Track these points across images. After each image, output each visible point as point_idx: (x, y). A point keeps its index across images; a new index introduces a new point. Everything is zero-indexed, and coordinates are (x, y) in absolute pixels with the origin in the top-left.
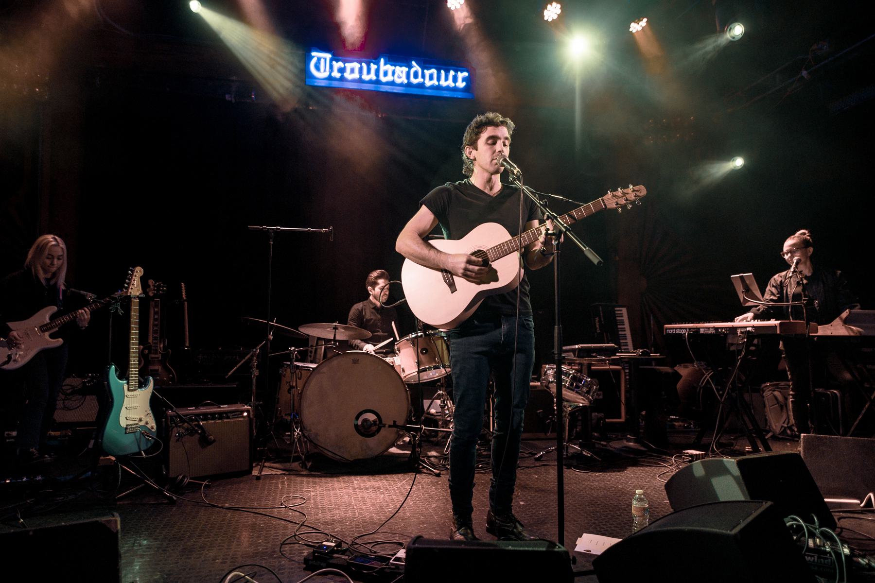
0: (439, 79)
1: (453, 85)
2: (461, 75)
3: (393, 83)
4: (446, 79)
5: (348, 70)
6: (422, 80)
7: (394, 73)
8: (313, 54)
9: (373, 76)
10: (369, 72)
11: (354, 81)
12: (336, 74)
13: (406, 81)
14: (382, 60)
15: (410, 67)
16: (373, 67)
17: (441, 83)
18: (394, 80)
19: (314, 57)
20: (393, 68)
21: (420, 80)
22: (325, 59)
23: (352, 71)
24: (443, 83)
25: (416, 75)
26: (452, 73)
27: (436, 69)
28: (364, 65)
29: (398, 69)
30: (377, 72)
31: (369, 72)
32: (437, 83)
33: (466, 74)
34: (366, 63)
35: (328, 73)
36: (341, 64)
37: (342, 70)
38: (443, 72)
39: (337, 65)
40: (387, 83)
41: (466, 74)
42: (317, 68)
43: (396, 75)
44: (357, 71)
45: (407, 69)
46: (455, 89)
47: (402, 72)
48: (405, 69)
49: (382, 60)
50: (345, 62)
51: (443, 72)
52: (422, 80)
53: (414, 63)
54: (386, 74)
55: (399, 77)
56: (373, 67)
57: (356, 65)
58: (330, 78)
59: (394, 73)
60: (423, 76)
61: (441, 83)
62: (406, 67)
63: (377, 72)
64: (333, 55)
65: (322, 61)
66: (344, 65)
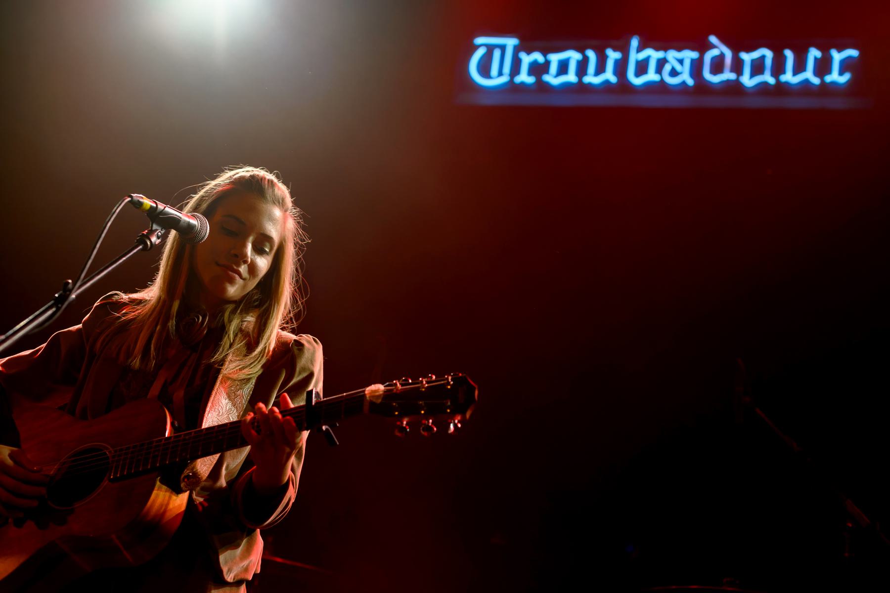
0: (778, 68)
1: (816, 81)
2: (837, 56)
3: (660, 87)
4: (799, 67)
5: (554, 68)
6: (732, 76)
7: (661, 63)
8: (479, 41)
9: (609, 75)
10: (601, 69)
11: (567, 88)
12: (524, 77)
13: (690, 82)
14: (635, 42)
15: (703, 47)
16: (613, 56)
17: (784, 78)
18: (662, 81)
19: (477, 47)
20: (660, 54)
21: (728, 75)
22: (503, 48)
23: (563, 68)
24: (788, 77)
25: (718, 66)
26: (814, 53)
27: (769, 47)
28: (591, 54)
29: (672, 55)
30: (621, 68)
31: (601, 69)
32: (771, 81)
33: (853, 53)
34: (593, 48)
35: (504, 79)
36: (538, 57)
37: (538, 70)
38: (789, 54)
39: (527, 59)
40: (650, 88)
41: (853, 53)
42: (485, 69)
43: (667, 68)
44: (572, 67)
45: (694, 55)
46: (826, 90)
47: (681, 62)
48: (689, 55)
49: (635, 42)
50: (545, 53)
51: (789, 54)
52: (732, 76)
53: (713, 39)
54: (642, 68)
55: (674, 73)
56: (613, 56)
57: (574, 56)
58: (512, 88)
59: (661, 63)
60: (737, 66)
61: (784, 78)
62: (693, 49)
63: (621, 68)
64: (522, 38)
65: (497, 54)
66: (545, 55)
